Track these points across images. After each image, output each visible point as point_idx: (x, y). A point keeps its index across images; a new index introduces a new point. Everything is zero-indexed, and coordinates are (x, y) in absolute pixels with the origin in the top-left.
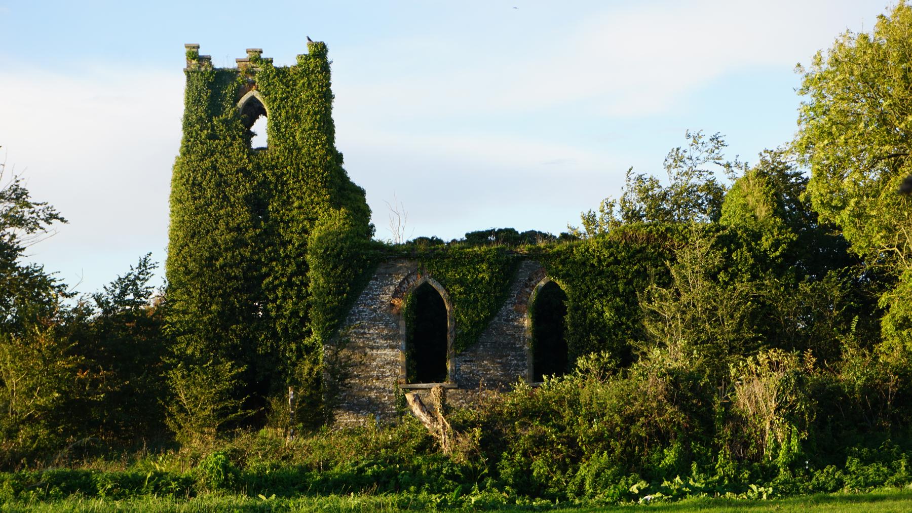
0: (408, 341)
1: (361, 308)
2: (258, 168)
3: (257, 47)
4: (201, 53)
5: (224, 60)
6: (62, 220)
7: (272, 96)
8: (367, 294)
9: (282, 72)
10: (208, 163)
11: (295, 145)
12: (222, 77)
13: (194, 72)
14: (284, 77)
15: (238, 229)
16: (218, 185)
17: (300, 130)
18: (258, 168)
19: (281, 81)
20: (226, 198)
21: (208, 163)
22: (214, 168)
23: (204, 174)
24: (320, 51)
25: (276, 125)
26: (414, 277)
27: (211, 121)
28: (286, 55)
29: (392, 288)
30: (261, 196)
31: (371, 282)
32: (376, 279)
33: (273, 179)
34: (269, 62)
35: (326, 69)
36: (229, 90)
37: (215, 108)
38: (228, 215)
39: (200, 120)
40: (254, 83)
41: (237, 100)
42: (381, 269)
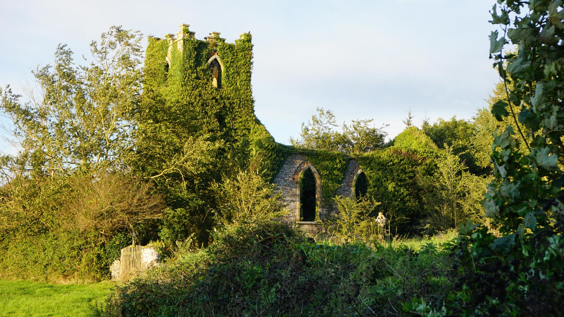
0: (301, 199)
1: (279, 179)
2: (222, 98)
3: (218, 31)
4: (191, 29)
5: (200, 36)
6: (370, 121)
7: (226, 59)
8: (283, 172)
9: (231, 47)
10: (196, 92)
11: (237, 88)
12: (201, 45)
13: (187, 40)
14: (232, 50)
15: (212, 131)
16: (202, 105)
17: (240, 80)
18: (222, 98)
19: (230, 52)
20: (206, 113)
21: (196, 92)
22: (200, 95)
23: (195, 98)
24: (249, 38)
25: (227, 76)
26: (303, 164)
27: (196, 69)
28: (232, 37)
29: (294, 169)
30: (222, 114)
31: (285, 166)
32: (287, 164)
33: (229, 105)
34: (224, 40)
35: (250, 48)
36: (205, 53)
37: (198, 63)
38: (208, 123)
39: (191, 67)
40: (216, 51)
41: (208, 60)
42: (289, 159)
